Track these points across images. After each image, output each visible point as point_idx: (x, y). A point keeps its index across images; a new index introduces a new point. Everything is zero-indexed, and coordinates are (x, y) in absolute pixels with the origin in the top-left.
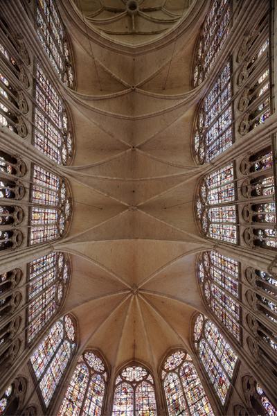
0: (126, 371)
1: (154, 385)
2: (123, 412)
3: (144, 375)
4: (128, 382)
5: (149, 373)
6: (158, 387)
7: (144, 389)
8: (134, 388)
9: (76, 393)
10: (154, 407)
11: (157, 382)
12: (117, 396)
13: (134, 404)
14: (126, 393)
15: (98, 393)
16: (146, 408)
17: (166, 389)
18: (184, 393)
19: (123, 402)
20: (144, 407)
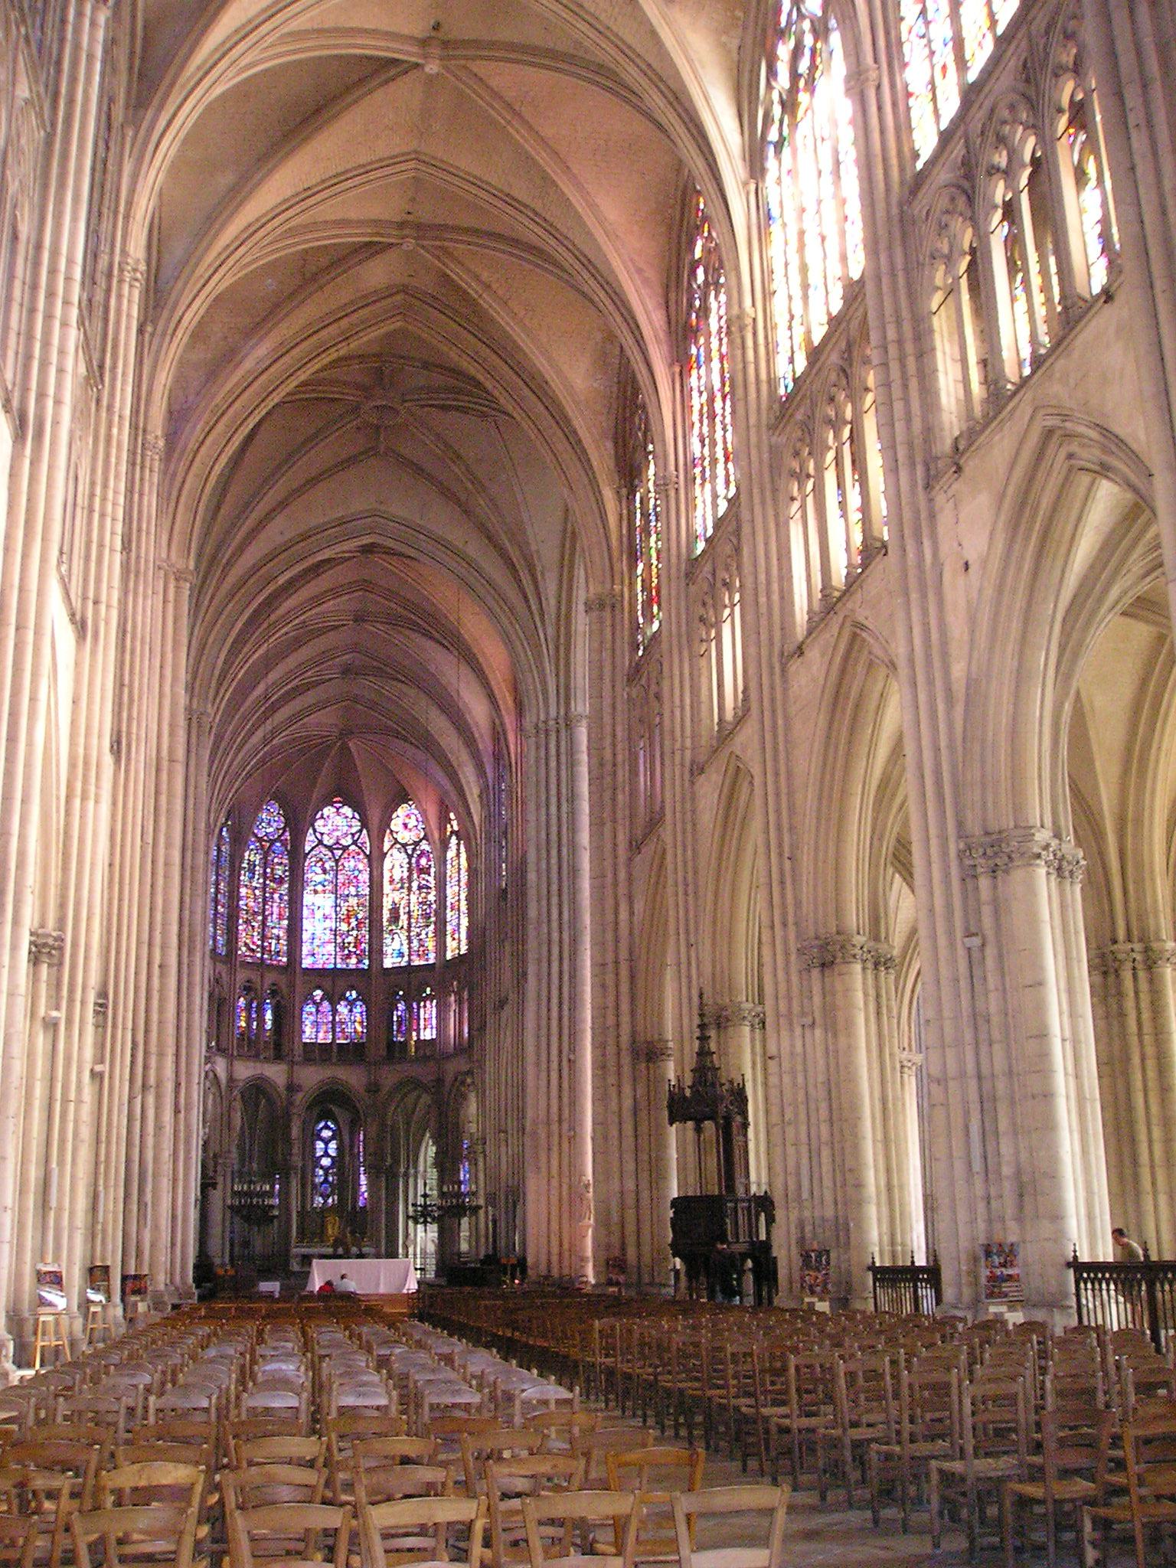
0: (322, 817)
1: (367, 856)
3: (354, 830)
5: (364, 824)
6: (375, 864)
7: (352, 863)
8: (337, 861)
9: (252, 904)
11: (375, 854)
12: (309, 876)
13: (335, 892)
14: (325, 871)
15: (281, 881)
16: (353, 901)
19: (319, 888)
20: (350, 899)
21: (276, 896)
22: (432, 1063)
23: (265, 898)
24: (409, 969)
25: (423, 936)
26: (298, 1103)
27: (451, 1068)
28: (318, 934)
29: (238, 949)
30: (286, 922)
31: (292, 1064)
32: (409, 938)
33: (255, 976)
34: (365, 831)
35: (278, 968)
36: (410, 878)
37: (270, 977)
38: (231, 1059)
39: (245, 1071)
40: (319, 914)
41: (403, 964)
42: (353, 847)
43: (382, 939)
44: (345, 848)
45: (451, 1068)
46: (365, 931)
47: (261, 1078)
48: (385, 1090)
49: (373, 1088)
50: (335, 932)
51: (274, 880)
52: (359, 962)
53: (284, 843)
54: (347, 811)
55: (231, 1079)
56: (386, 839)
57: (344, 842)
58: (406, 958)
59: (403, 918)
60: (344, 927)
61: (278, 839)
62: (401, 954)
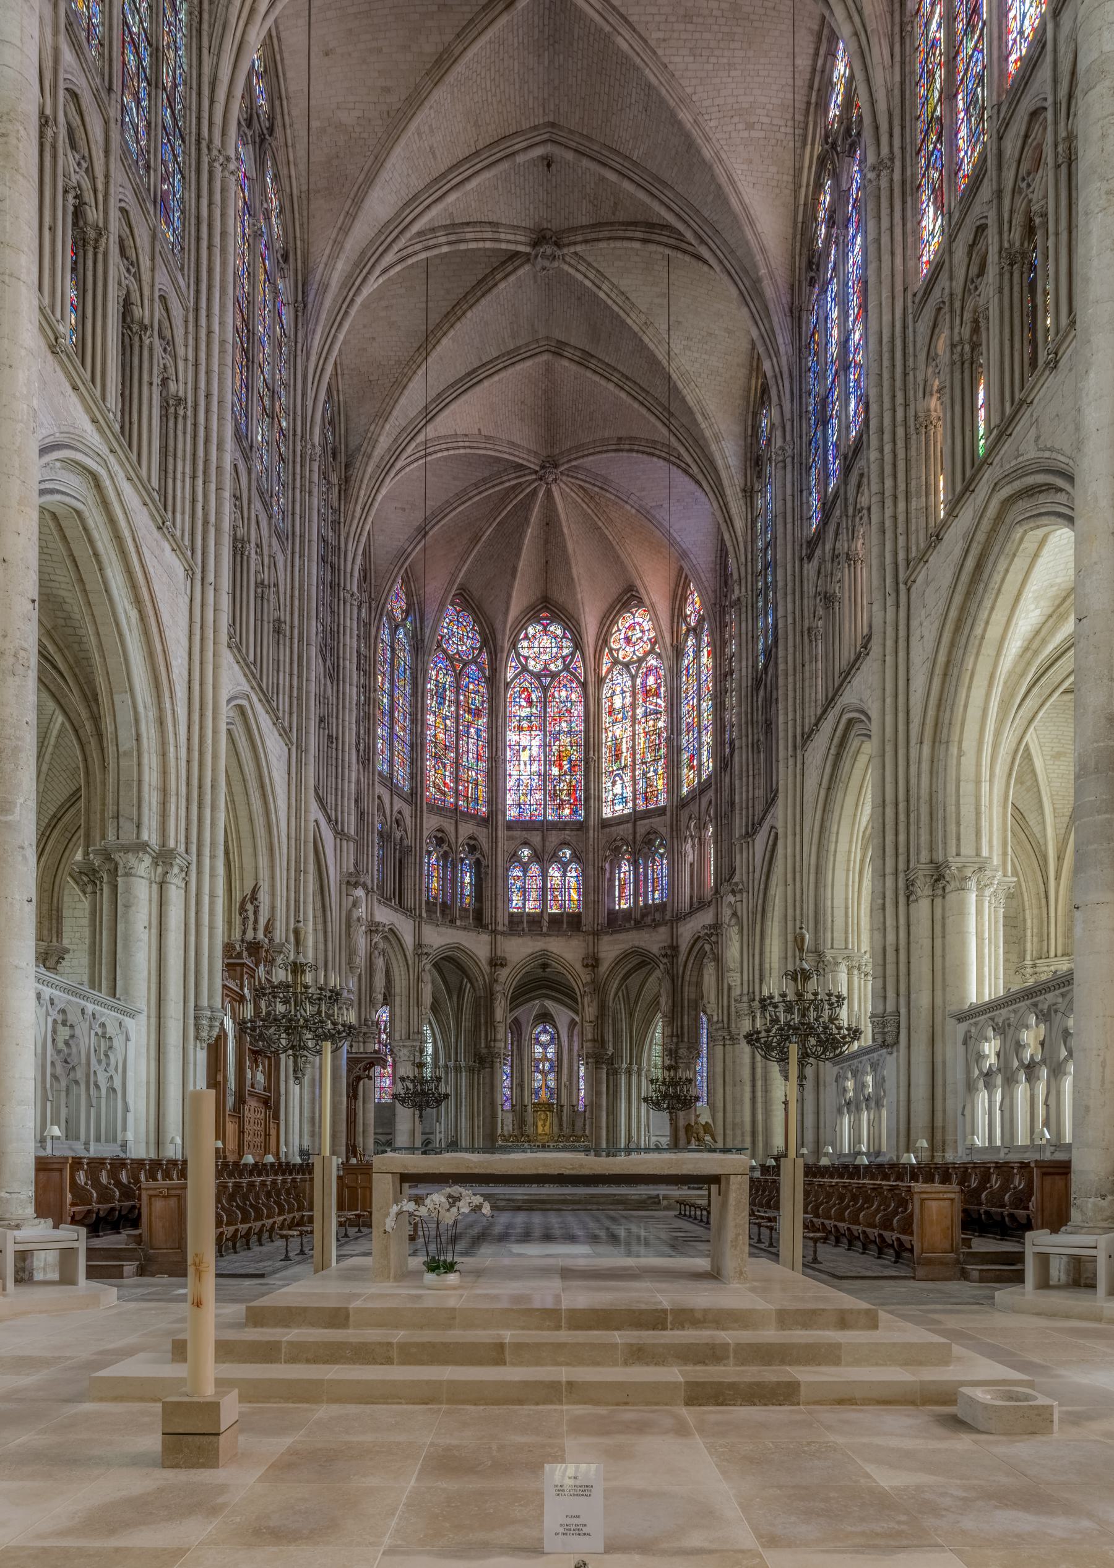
0: (526, 637)
1: (584, 685)
2: (525, 748)
3: (565, 652)
4: (531, 673)
5: (578, 645)
6: (591, 689)
7: (564, 694)
8: (545, 689)
10: (580, 738)
11: (591, 678)
14: (530, 703)
15: (477, 713)
16: (565, 740)
17: (605, 704)
18: (634, 735)
20: (562, 737)
21: (472, 730)
22: (663, 930)
23: (457, 732)
24: (636, 817)
25: (651, 774)
26: (502, 979)
27: (687, 931)
28: (525, 779)
29: (428, 789)
30: (482, 765)
31: (494, 932)
32: (633, 778)
33: (450, 828)
34: (578, 653)
35: (473, 817)
36: (633, 706)
37: (467, 829)
38: (418, 921)
39: (437, 938)
40: (524, 756)
41: (626, 811)
42: (564, 674)
43: (600, 782)
44: (554, 675)
45: (687, 931)
46: (579, 775)
47: (458, 948)
48: (604, 968)
49: (592, 962)
50: (544, 776)
51: (469, 711)
52: (573, 812)
53: (480, 669)
54: (556, 629)
55: (419, 945)
56: (605, 660)
57: (552, 667)
58: (630, 805)
59: (626, 754)
60: (555, 771)
61: (474, 661)
62: (624, 800)
